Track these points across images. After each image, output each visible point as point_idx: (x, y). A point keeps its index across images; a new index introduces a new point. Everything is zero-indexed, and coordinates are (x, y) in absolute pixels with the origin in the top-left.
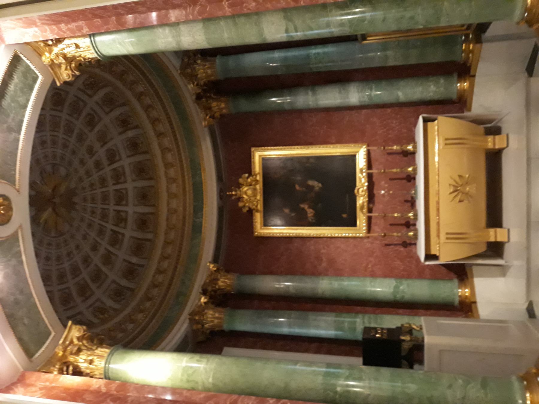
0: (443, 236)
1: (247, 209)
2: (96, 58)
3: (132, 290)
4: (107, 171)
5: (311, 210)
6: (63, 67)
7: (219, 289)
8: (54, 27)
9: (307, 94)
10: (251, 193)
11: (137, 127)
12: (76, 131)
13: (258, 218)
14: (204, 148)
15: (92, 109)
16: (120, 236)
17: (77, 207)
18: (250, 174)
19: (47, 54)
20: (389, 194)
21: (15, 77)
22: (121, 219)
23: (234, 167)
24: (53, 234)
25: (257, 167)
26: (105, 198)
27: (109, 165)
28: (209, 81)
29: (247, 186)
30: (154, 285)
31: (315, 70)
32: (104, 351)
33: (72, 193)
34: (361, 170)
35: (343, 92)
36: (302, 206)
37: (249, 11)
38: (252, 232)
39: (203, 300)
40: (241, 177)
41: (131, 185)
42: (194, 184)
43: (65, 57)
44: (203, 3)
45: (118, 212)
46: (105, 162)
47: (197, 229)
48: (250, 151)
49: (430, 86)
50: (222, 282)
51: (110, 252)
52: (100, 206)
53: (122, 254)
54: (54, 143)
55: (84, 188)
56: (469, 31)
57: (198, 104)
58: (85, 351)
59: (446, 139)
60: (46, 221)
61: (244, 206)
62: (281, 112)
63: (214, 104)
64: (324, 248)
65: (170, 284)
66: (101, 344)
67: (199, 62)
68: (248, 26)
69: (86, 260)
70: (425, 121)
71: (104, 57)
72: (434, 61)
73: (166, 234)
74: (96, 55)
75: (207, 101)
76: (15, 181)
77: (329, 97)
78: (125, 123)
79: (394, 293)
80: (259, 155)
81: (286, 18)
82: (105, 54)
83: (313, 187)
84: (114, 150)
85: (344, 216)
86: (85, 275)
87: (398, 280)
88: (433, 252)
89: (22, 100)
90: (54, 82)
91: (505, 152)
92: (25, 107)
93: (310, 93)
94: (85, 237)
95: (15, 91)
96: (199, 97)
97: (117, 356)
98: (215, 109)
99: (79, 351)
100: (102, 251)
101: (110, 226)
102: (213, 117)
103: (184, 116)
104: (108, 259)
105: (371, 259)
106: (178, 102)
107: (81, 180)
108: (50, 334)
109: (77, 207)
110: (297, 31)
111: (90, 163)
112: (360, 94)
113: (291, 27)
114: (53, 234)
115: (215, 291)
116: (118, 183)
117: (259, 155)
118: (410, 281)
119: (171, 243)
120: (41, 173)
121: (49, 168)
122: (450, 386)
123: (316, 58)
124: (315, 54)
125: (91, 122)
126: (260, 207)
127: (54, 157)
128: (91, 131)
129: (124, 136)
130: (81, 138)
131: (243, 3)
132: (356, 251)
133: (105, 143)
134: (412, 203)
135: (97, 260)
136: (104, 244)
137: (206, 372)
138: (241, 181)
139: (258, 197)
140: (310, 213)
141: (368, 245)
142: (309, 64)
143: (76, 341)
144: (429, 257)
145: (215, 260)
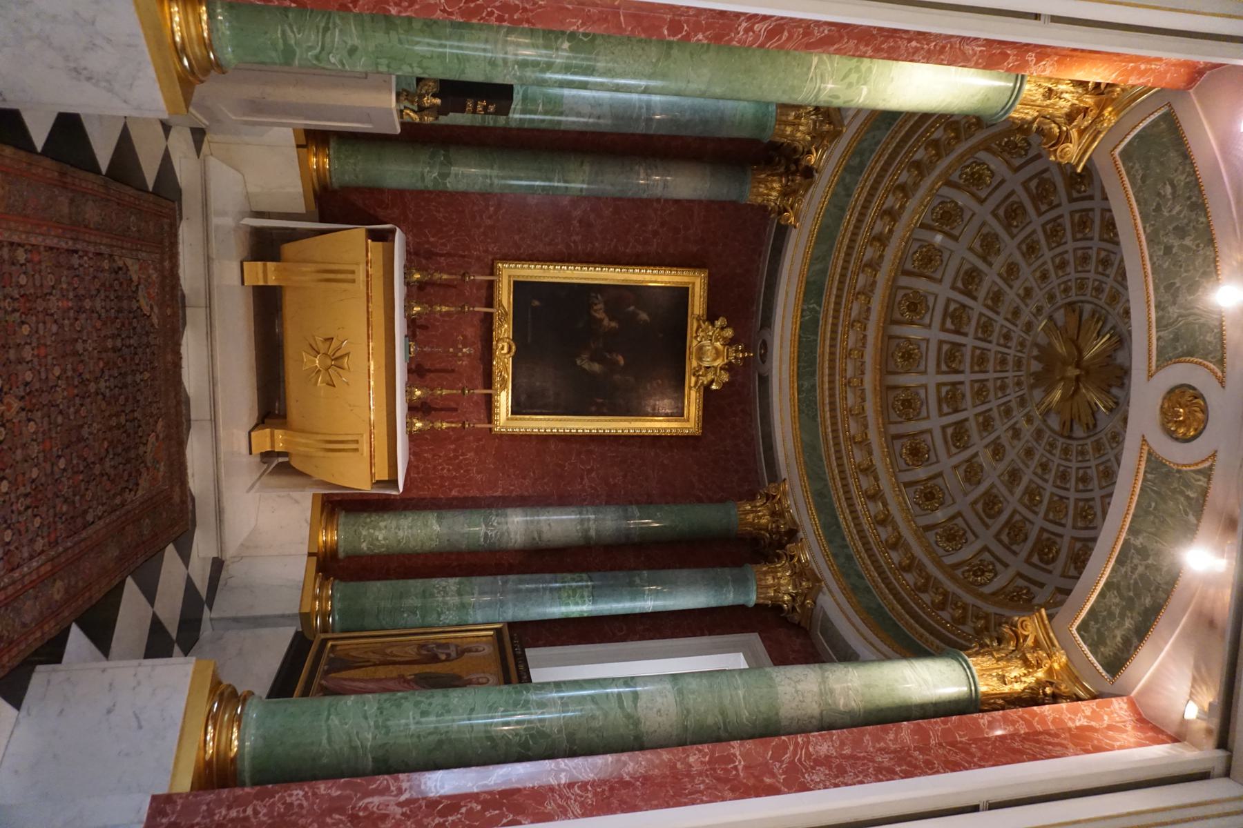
0: (361, 276)
1: (718, 323)
2: (969, 656)
3: (948, 183)
4: (970, 412)
5: (598, 316)
6: (1030, 642)
7: (781, 175)
8: (1039, 728)
9: (597, 531)
10: (709, 351)
11: (908, 485)
12: (1019, 491)
13: (697, 305)
14: (790, 445)
15: (987, 526)
16: (960, 284)
17: (1035, 352)
18: (707, 388)
19: (1056, 666)
20: (454, 346)
21: (1119, 639)
22: (956, 318)
23: (735, 404)
24: (1088, 308)
25: (693, 402)
26: (981, 361)
27: (966, 420)
28: (772, 562)
29: (716, 368)
30: (904, 190)
31: (584, 576)
32: (1021, 113)
33: (1044, 380)
34: (504, 387)
35: (536, 535)
36: (613, 324)
37: (700, 747)
38: (710, 276)
39: (813, 159)
40: (725, 385)
41: (933, 422)
42: (813, 374)
43: (1026, 663)
44: (778, 764)
45: (957, 332)
46: (972, 426)
47: (813, 290)
48: (703, 428)
49: (385, 539)
50: (773, 189)
51: (985, 259)
52: (993, 347)
53: (959, 252)
54: (1064, 476)
55: (1019, 384)
56: (323, 636)
57: (794, 522)
58: (1057, 113)
59: (356, 450)
60: (1099, 335)
61: (722, 328)
62: (647, 501)
63: (763, 521)
64: (575, 242)
65: (874, 188)
66: (1023, 128)
67: (786, 598)
68: (702, 709)
69: (1031, 249)
70: (393, 482)
71: (955, 657)
72: (379, 584)
73: (874, 283)
74: (970, 660)
75: (778, 527)
76: (1148, 460)
77: (560, 524)
78: (930, 495)
79: (450, 163)
80: (690, 422)
81: (637, 723)
82: (955, 664)
83: (592, 359)
84: (954, 445)
85: (536, 303)
86: (1036, 222)
87: (440, 188)
88: (376, 248)
89: (1113, 599)
90: (1050, 617)
91: (254, 421)
92: (1108, 585)
93: (592, 533)
94: (1028, 292)
95: (1122, 616)
96: (792, 534)
97: (997, 103)
98: (763, 511)
99: (1070, 117)
100: (999, 262)
101: (977, 308)
102: (769, 497)
103: (822, 503)
104: (989, 245)
105: (489, 222)
106: (831, 530)
107: (1022, 402)
108: (1122, 154)
109: (1035, 352)
110: (619, 695)
111: (1001, 429)
112: (505, 527)
113: (628, 704)
114: (1088, 308)
115: (788, 172)
116: (954, 384)
117: (690, 422)
118: (420, 186)
119: (866, 265)
120: (1095, 426)
121: (1079, 432)
122: (352, 51)
123: (582, 597)
124: (584, 603)
125: (991, 503)
126: (692, 325)
127: (1066, 451)
128: (993, 486)
129: (934, 470)
130: (1014, 476)
131: (709, 762)
132: (517, 237)
133: (968, 460)
134: (413, 325)
135: (1010, 247)
136: (992, 276)
137: (822, 76)
138: (725, 377)
139: (695, 343)
140: (599, 312)
141: (493, 248)
142: (593, 587)
143: (1074, 134)
144: (383, 237)
145: (783, 232)
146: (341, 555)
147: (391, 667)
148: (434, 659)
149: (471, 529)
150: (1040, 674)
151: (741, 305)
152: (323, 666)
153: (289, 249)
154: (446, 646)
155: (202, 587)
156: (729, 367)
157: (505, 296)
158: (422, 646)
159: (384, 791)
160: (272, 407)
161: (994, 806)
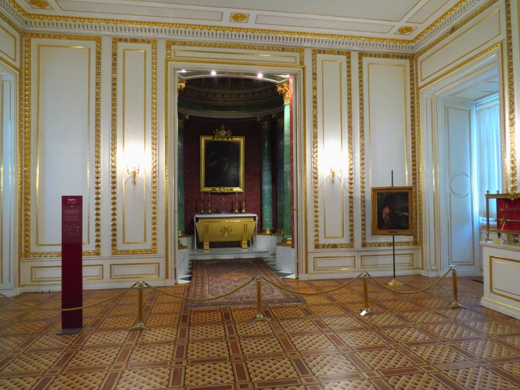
0: (207, 223)
13: (210, 138)
70: (254, 218)
77: (267, 177)
93: (269, 168)
140: (212, 165)
144: (197, 219)
149: (267, 198)
151: (210, 126)
153: (201, 240)
156: (226, 130)
157: (209, 189)
160: (237, 244)
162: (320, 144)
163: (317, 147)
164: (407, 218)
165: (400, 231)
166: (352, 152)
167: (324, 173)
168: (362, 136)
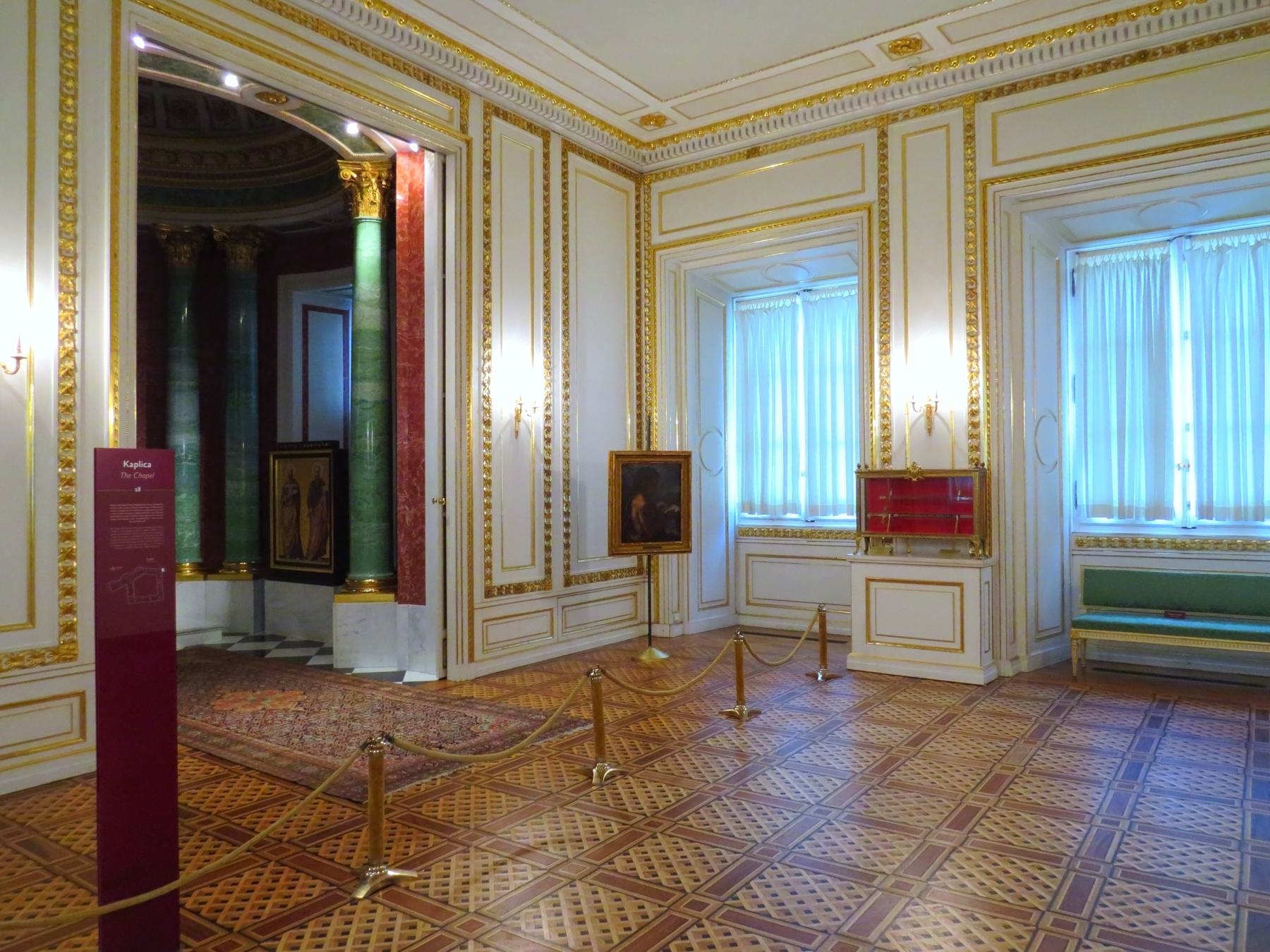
93: (192, 384)
146: (200, 560)
147: (301, 522)
148: (296, 498)
150: (373, 180)
152: (298, 560)
154: (285, 491)
155: (240, 638)
158: (284, 504)
159: (404, 516)
161: (444, 272)
162: (494, 341)
163: (490, 347)
164: (678, 517)
165: (666, 546)
166: (549, 368)
167: (502, 411)
168: (566, 334)
